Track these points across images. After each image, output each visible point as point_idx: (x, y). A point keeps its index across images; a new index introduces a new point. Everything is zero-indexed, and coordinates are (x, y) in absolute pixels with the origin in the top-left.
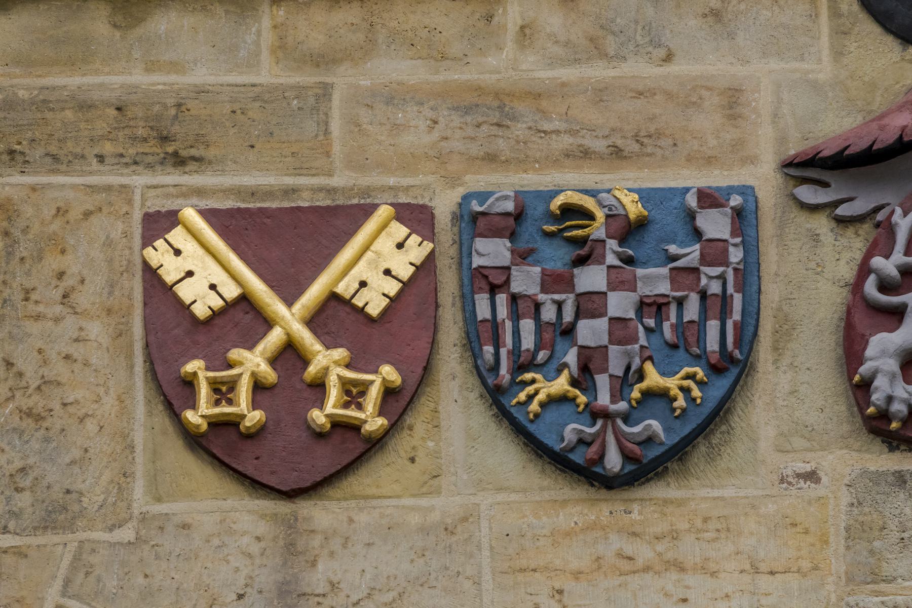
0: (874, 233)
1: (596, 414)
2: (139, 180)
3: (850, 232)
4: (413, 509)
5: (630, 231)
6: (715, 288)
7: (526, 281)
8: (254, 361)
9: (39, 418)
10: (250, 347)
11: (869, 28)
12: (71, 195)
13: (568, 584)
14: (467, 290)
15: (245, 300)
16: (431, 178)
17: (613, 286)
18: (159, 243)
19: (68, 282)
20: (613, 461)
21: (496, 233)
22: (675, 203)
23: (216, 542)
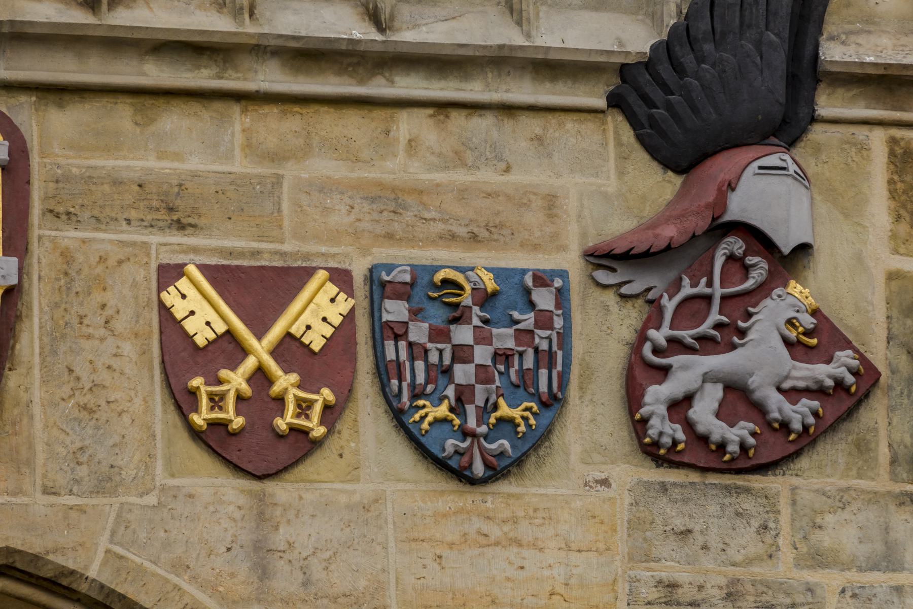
0: (647, 308)
1: (465, 434)
2: (154, 239)
3: (629, 304)
4: (341, 491)
5: (486, 299)
6: (544, 346)
7: (418, 333)
8: (237, 380)
9: (91, 411)
10: (233, 368)
11: (641, 156)
12: (109, 247)
13: (446, 553)
14: (378, 336)
15: (230, 334)
16: (350, 249)
17: (478, 341)
18: (171, 289)
19: (109, 312)
20: (479, 469)
21: (398, 296)
22: (516, 279)
23: (212, 509)
